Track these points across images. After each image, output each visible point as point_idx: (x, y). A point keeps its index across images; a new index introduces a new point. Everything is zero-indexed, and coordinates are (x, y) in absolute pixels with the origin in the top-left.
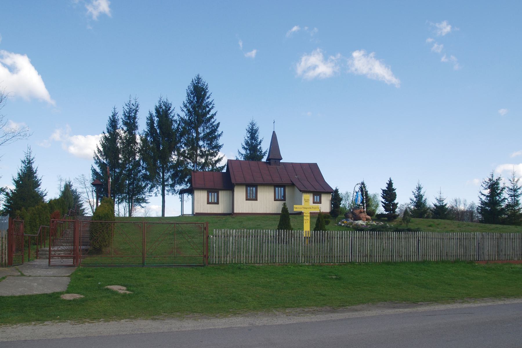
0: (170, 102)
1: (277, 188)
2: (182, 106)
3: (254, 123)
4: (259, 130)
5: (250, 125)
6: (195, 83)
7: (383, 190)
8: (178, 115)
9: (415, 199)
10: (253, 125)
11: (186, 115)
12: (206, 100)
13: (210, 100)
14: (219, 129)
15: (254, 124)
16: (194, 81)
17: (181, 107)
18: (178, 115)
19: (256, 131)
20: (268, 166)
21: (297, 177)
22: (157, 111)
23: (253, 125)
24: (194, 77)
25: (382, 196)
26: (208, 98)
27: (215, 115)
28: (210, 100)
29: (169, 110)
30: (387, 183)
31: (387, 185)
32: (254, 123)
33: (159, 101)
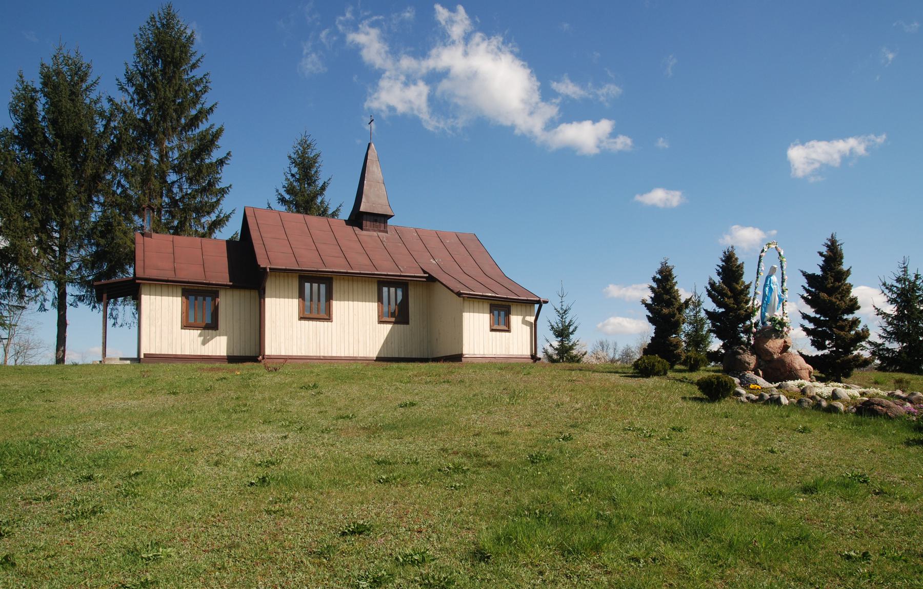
0: (85, 61)
1: (385, 289)
2: (123, 80)
3: (308, 143)
4: (319, 160)
5: (299, 147)
6: (159, 25)
7: (811, 278)
8: (110, 100)
9: (891, 309)
10: (305, 146)
11: (132, 101)
12: (189, 72)
13: (197, 73)
14: (220, 142)
15: (308, 146)
16: (157, 19)
17: (117, 80)
18: (110, 100)
19: (315, 160)
20: (356, 232)
21: (434, 262)
22: (47, 80)
23: (305, 146)
24: (157, 10)
25: (803, 297)
26: (194, 66)
27: (212, 111)
28: (197, 73)
29: (82, 80)
30: (821, 254)
31: (821, 261)
32: (308, 143)
33: (55, 56)
